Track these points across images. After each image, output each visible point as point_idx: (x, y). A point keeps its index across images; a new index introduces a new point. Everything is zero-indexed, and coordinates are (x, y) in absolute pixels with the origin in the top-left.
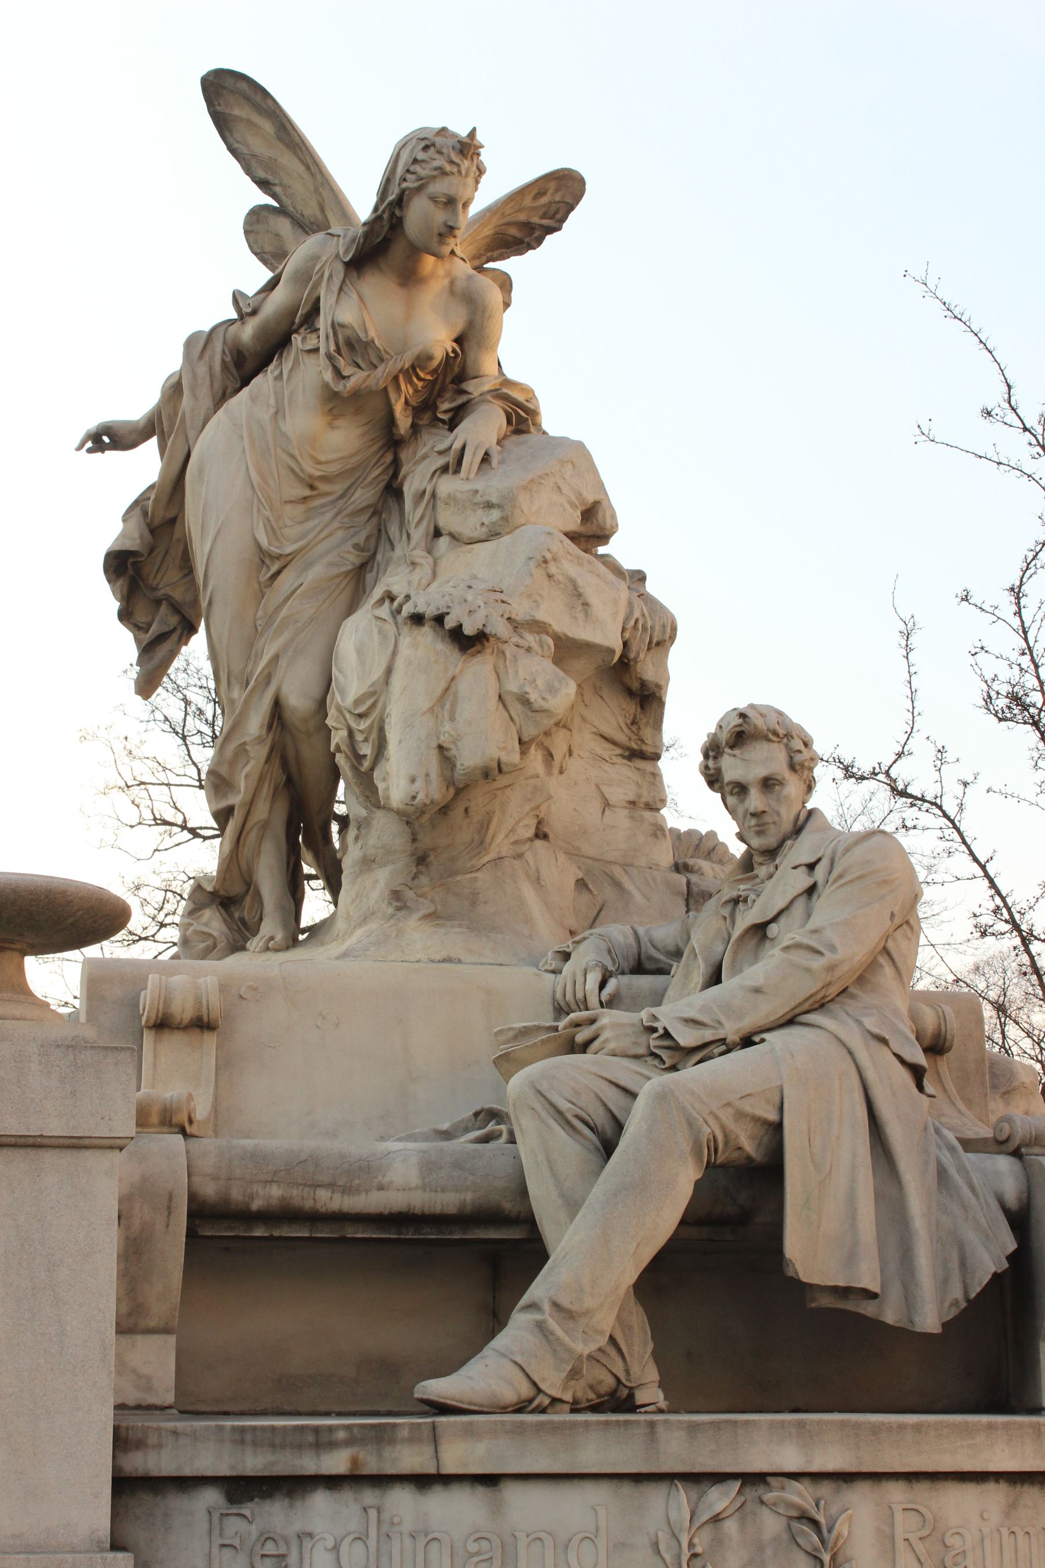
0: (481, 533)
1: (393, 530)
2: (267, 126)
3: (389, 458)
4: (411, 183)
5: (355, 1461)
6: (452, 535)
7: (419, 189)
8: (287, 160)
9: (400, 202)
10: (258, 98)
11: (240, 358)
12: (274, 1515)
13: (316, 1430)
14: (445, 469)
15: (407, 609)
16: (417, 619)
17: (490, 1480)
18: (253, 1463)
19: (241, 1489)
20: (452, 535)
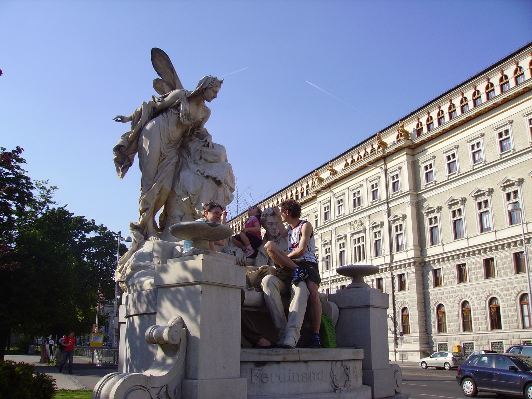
0: (213, 161)
1: (185, 155)
2: (165, 62)
3: (182, 139)
4: (210, 86)
5: (284, 358)
6: (205, 160)
7: (210, 88)
8: (169, 71)
9: (205, 89)
10: (165, 57)
11: (155, 111)
12: (267, 369)
13: (277, 352)
14: (204, 145)
15: (206, 174)
16: (208, 177)
17: (306, 362)
18: (263, 358)
19: (260, 364)
20: (205, 160)
